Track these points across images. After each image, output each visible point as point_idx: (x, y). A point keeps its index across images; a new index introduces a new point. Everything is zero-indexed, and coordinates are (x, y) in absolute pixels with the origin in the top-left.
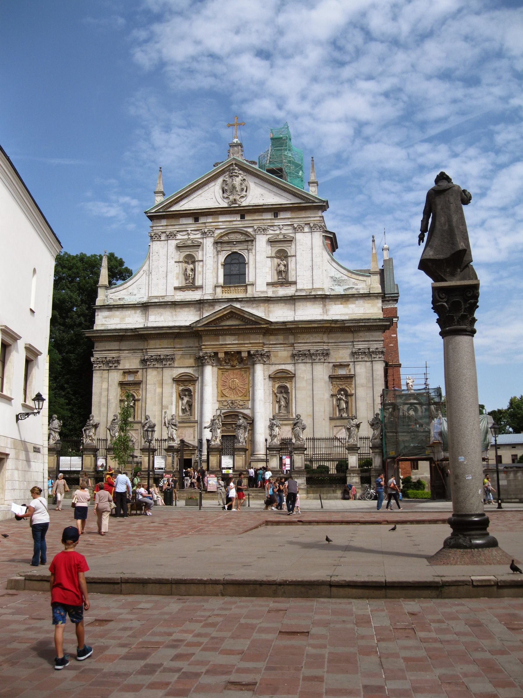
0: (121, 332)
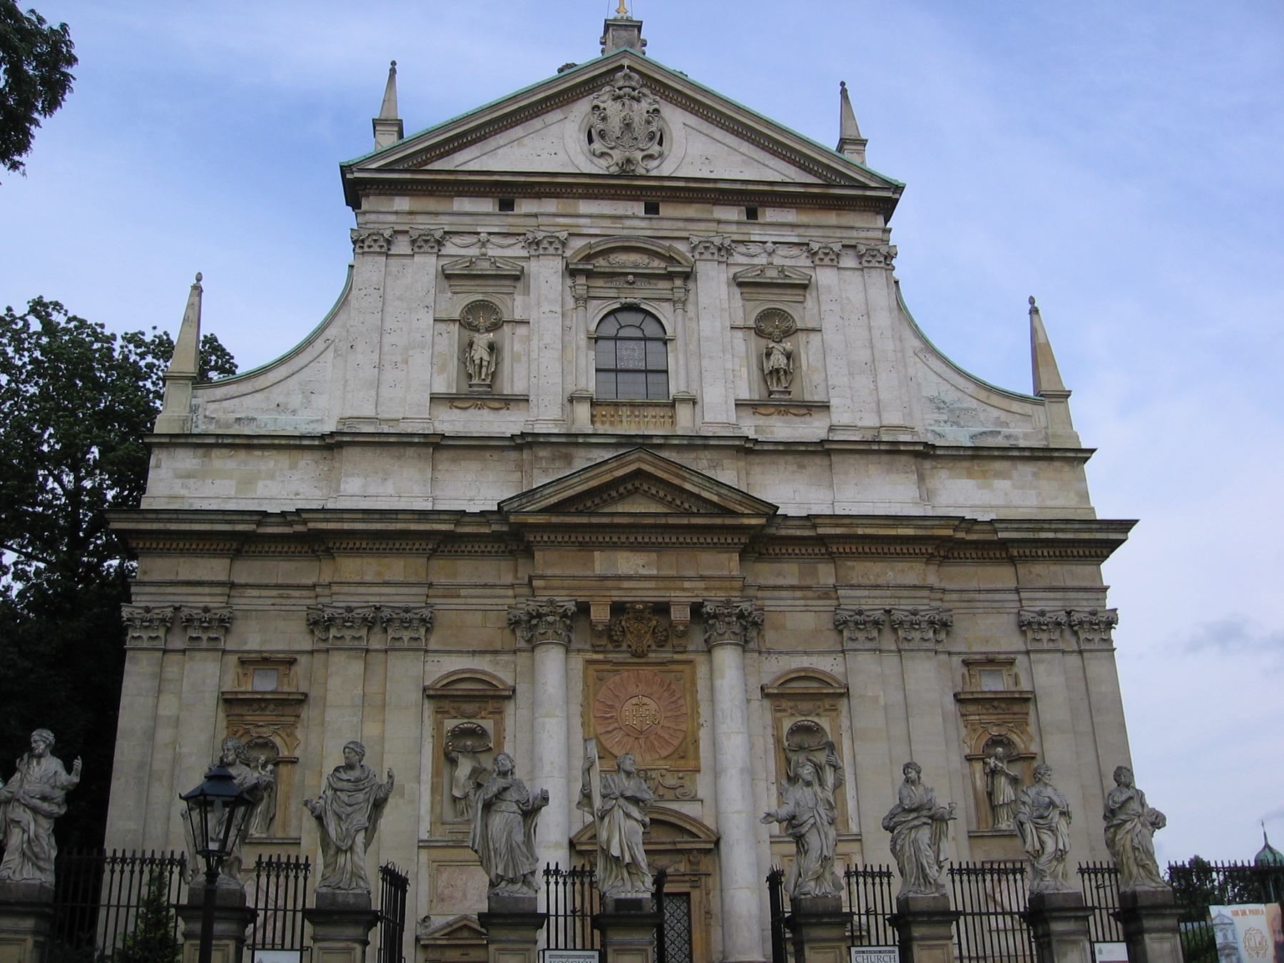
0: (243, 522)
